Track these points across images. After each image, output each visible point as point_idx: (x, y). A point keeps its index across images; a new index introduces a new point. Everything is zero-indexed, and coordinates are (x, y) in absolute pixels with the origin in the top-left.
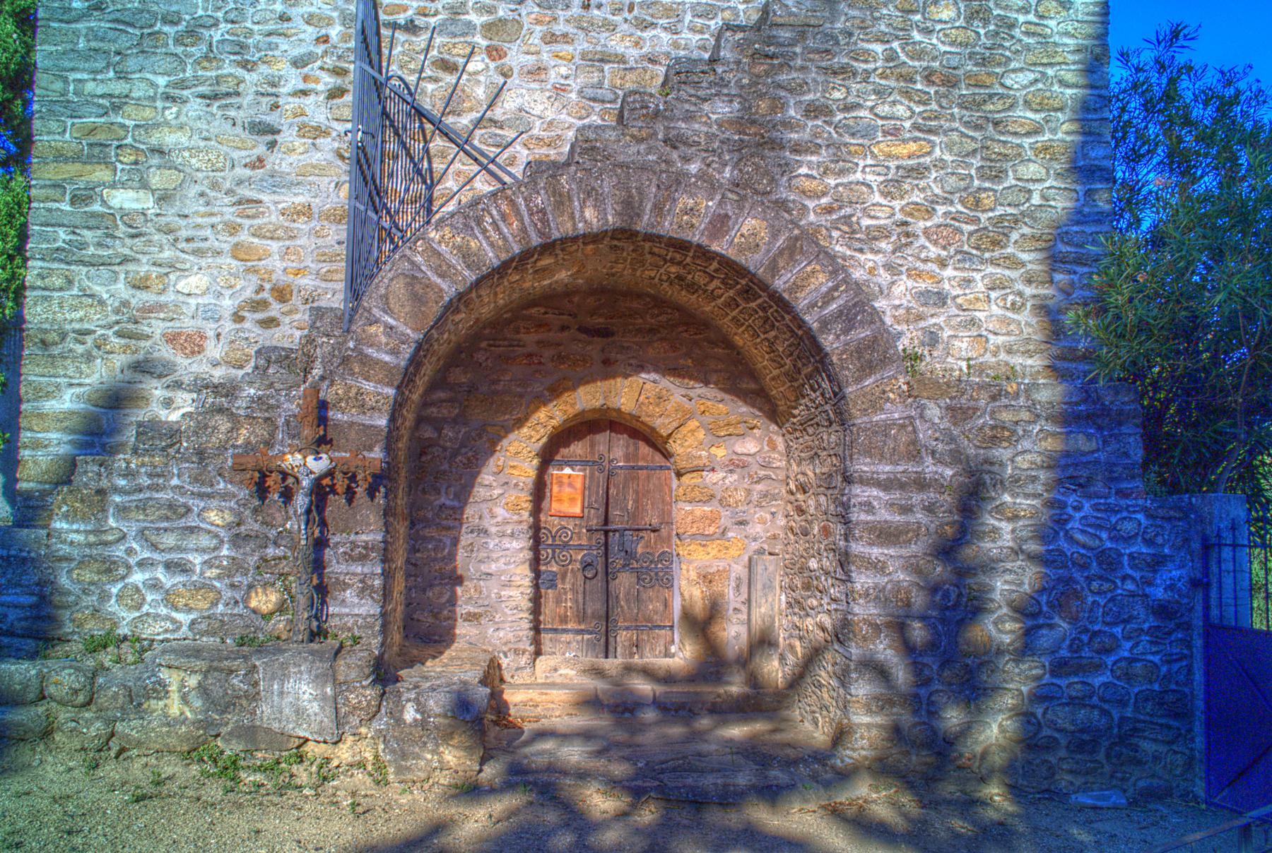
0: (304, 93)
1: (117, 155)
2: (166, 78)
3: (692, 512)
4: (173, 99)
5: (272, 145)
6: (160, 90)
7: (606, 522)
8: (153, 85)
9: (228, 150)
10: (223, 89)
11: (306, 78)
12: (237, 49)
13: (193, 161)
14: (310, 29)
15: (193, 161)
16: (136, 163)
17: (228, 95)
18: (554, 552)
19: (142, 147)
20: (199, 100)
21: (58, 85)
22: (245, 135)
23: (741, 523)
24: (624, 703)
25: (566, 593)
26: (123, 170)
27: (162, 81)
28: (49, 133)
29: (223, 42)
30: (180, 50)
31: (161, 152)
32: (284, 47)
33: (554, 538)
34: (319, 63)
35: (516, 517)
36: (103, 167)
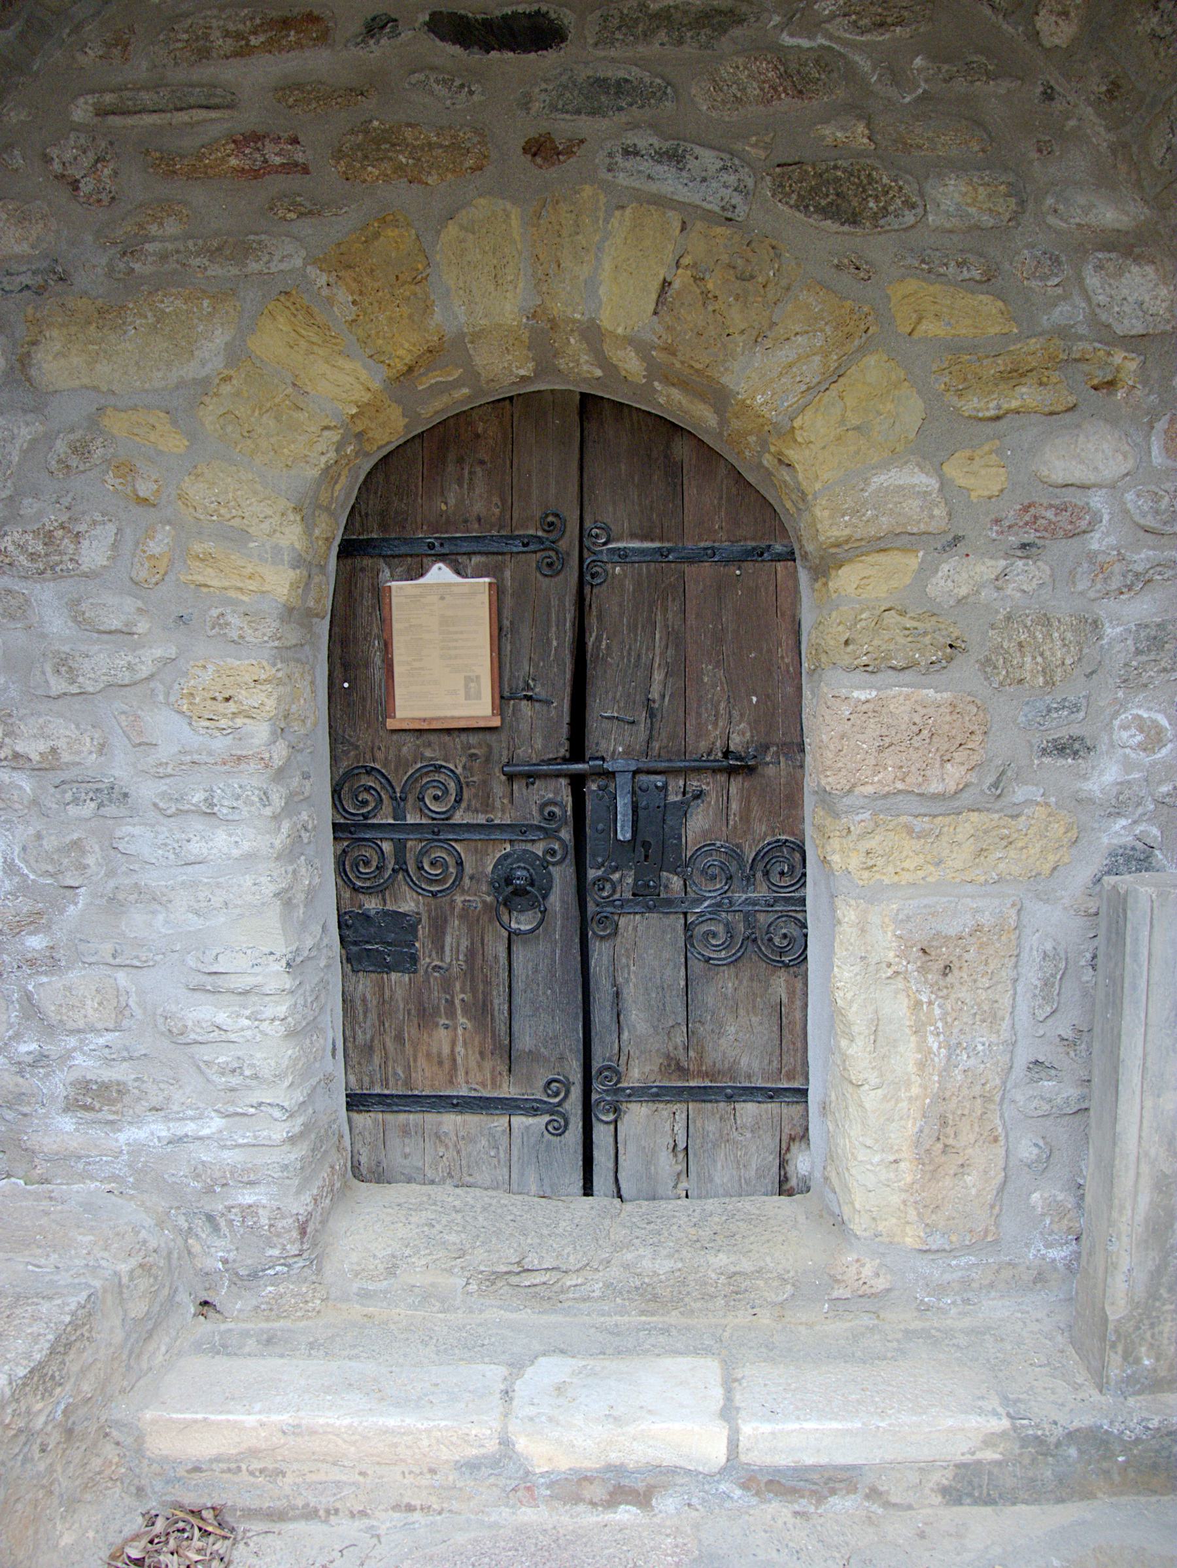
3: (876, 709)
7: (577, 746)
18: (400, 848)
23: (1062, 749)
24: (618, 1469)
25: (447, 986)
33: (399, 802)
35: (220, 744)
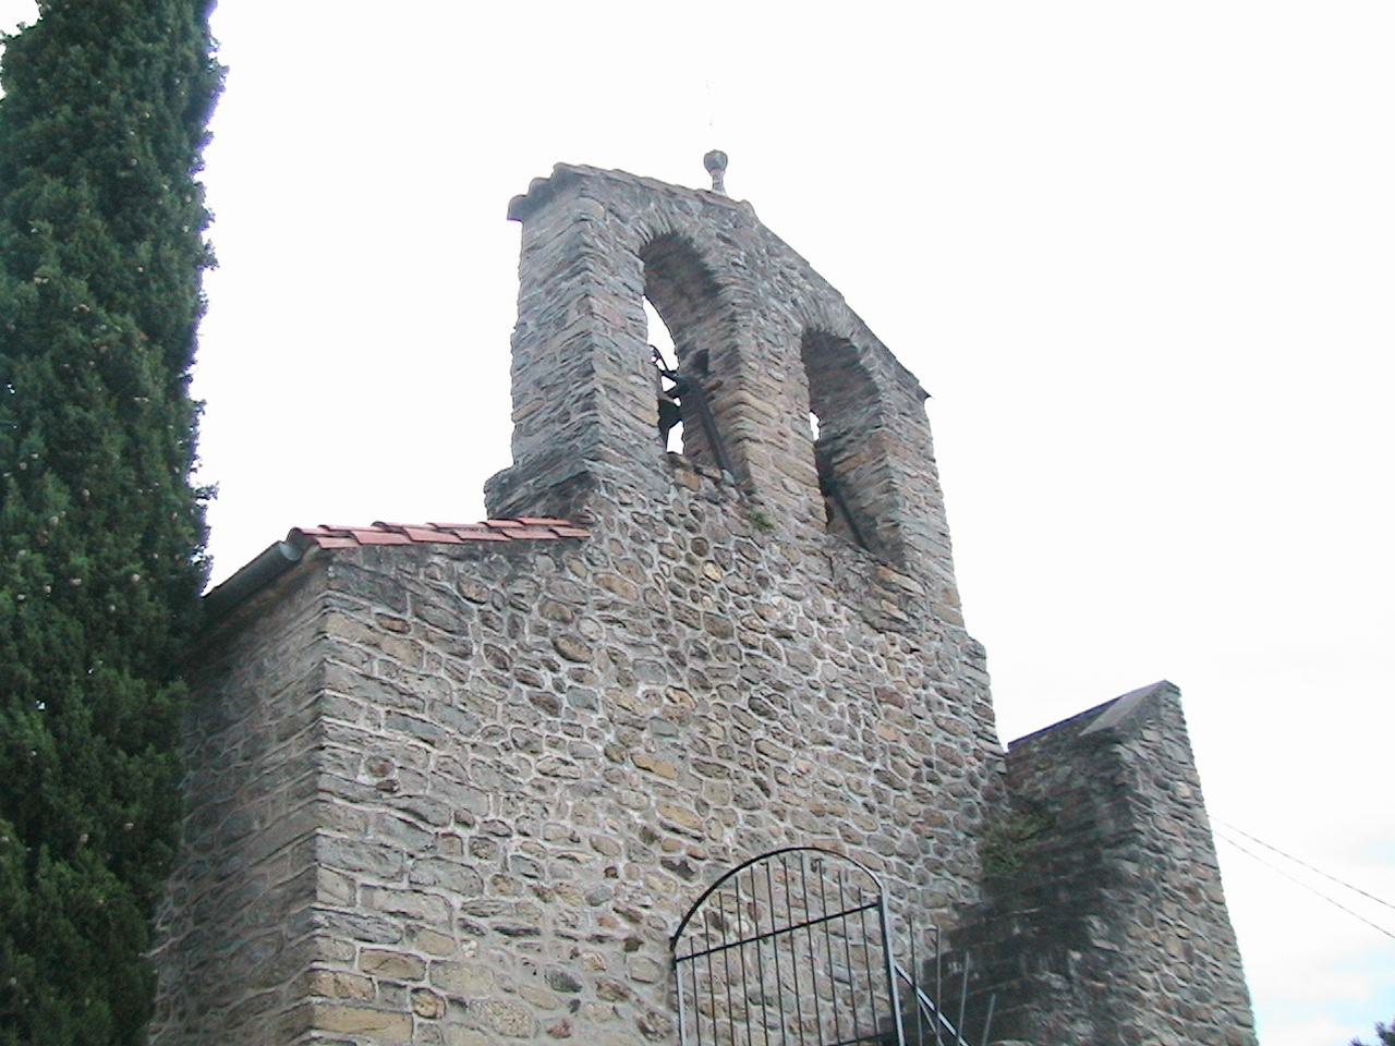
0: (600, 939)
1: (414, 1002)
2: (462, 899)
4: (466, 927)
5: (575, 1005)
6: (458, 914)
8: (449, 906)
9: (531, 1007)
10: (524, 923)
11: (601, 922)
12: (533, 872)
13: (497, 1020)
14: (599, 857)
15: (497, 1020)
16: (433, 1017)
17: (528, 932)
19: (442, 993)
20: (497, 934)
21: (344, 889)
22: (547, 989)
26: (420, 1025)
27: (457, 901)
28: (336, 959)
29: (516, 858)
30: (475, 861)
31: (460, 1003)
32: (576, 876)
34: (611, 904)
36: (398, 1018)
